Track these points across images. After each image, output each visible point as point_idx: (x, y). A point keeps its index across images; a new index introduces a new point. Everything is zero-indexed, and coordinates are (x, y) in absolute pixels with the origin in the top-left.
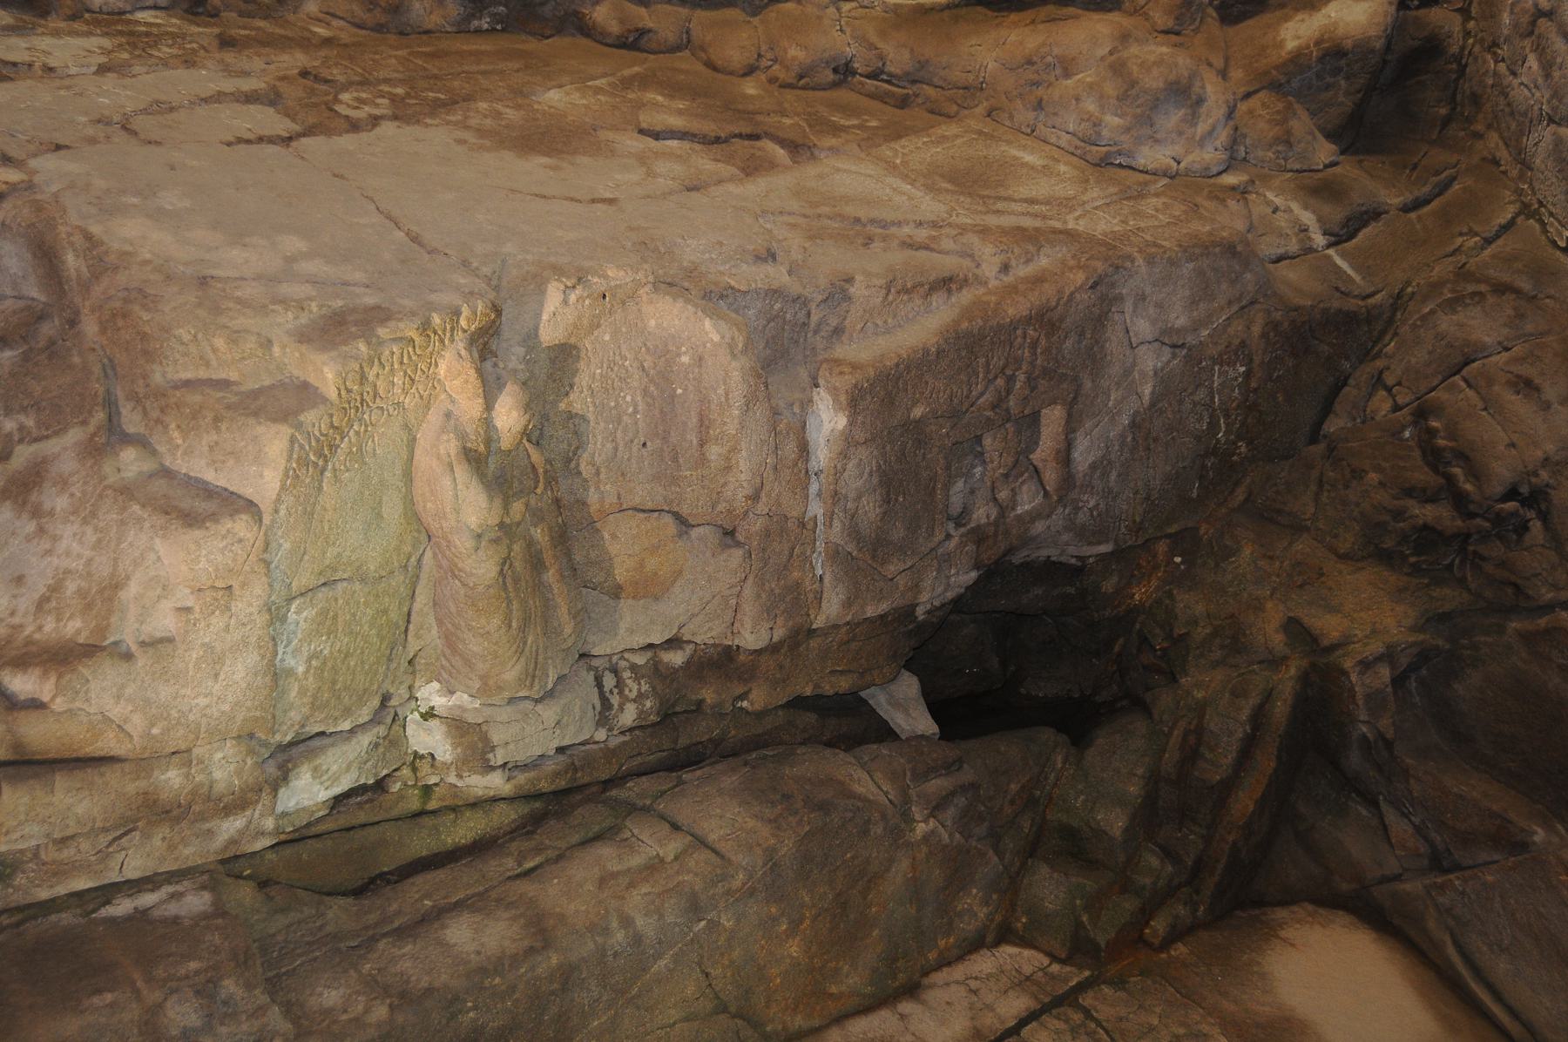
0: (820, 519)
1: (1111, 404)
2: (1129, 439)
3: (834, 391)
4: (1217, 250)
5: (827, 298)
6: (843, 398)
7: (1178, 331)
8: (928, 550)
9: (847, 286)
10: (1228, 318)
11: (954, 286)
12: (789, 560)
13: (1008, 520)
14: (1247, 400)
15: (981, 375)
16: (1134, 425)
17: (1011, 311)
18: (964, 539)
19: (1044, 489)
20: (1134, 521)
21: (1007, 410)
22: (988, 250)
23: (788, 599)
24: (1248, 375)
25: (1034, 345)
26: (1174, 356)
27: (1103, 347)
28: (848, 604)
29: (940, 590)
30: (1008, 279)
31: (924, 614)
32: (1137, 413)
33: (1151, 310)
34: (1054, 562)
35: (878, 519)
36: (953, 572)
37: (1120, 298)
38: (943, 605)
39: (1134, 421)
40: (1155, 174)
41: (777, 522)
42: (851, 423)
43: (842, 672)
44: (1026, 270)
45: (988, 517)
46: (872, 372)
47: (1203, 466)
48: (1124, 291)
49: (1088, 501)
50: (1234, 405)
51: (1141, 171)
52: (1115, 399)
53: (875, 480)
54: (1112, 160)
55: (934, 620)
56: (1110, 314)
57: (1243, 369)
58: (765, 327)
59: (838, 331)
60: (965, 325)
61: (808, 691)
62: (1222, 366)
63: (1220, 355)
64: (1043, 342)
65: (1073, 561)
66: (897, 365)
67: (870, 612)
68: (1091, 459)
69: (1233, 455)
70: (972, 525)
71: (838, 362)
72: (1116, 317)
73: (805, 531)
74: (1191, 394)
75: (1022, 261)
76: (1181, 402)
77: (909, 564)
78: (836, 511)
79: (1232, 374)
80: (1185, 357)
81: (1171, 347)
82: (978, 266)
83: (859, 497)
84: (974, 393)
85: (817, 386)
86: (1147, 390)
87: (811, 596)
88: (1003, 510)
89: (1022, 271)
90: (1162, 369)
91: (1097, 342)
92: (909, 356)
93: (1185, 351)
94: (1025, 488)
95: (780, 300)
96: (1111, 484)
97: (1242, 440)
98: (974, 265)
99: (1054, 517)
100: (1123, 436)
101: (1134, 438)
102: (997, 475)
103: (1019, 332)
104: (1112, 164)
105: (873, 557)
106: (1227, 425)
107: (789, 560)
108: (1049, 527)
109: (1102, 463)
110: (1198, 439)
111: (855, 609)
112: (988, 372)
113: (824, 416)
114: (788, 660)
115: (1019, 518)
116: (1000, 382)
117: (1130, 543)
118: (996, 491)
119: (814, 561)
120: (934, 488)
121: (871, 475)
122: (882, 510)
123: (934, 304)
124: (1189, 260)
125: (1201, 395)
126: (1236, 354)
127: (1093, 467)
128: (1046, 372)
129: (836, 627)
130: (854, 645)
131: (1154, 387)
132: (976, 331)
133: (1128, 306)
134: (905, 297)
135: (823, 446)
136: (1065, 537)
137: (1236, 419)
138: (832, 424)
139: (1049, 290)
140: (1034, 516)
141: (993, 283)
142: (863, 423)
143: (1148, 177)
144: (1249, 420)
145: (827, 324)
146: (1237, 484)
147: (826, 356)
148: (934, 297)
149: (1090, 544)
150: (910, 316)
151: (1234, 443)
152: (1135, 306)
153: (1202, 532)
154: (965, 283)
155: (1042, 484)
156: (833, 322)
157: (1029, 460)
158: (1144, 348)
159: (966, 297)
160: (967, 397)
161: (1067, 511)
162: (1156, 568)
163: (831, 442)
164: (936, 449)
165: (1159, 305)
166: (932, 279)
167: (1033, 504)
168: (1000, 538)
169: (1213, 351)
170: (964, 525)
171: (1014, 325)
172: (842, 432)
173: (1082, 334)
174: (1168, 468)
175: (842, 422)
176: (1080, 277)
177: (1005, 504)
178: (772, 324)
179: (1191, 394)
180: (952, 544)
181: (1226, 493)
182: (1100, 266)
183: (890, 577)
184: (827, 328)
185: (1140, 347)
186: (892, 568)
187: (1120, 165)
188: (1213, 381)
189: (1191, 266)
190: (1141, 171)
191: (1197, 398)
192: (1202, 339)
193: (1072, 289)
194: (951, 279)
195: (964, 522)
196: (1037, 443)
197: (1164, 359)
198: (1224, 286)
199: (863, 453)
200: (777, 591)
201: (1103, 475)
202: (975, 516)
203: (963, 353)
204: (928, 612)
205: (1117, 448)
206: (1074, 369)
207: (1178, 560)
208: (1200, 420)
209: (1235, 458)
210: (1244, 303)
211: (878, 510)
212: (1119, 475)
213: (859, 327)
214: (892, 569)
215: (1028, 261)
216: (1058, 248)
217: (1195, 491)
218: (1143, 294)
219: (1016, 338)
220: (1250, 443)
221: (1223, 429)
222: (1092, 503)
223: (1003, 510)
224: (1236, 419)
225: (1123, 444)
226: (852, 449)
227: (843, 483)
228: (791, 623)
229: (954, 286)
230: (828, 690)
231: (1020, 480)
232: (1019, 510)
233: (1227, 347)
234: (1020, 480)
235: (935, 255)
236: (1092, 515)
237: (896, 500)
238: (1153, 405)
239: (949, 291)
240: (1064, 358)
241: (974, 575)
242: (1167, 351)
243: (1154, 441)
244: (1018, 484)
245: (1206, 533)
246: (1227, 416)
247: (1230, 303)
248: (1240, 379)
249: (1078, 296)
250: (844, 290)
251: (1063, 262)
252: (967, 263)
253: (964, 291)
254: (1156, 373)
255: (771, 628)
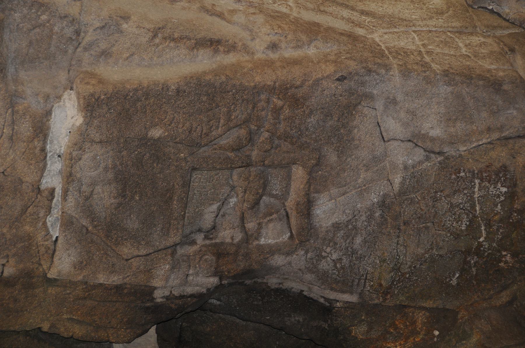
0: (58, 192)
1: (360, 181)
2: (377, 214)
3: (78, 94)
4: (481, 83)
5: (103, 27)
6: (82, 102)
7: (433, 140)
8: (162, 246)
9: (122, 22)
10: (490, 143)
11: (221, 48)
12: (21, 215)
13: (250, 246)
14: (509, 217)
15: (222, 121)
16: (383, 204)
17: (258, 79)
18: (204, 249)
19: (291, 233)
20: (381, 285)
21: (249, 157)
22: (266, 29)
23: (19, 245)
24: (511, 196)
25: (277, 111)
26: (428, 159)
27: (350, 131)
28: (79, 266)
29: (177, 282)
30: (273, 56)
31: (162, 298)
32: (385, 196)
33: (402, 115)
34: (305, 296)
35: (113, 206)
36: (191, 272)
37: (370, 97)
38: (182, 297)
39: (384, 202)
40: (513, 23)
41: (11, 181)
42: (88, 123)
43: (79, 322)
44: (293, 53)
45: (232, 238)
46: (110, 90)
47: (465, 262)
48: (375, 92)
49: (330, 253)
50: (496, 217)
51: (505, 19)
52: (364, 178)
53: (110, 175)
54: (487, 6)
55: (173, 306)
56: (359, 107)
57: (504, 190)
58: (30, 30)
59: (105, 54)
60: (208, 78)
61: (46, 327)
62: (482, 180)
63: (480, 171)
64: (287, 112)
65: (322, 300)
66: (136, 90)
67: (102, 279)
68: (334, 219)
69: (501, 261)
70: (217, 241)
71: (92, 75)
72: (366, 111)
73: (39, 196)
74: (448, 196)
75: (292, 45)
76: (435, 200)
77: (143, 252)
78: (71, 188)
79: (492, 190)
80: (440, 163)
81: (425, 150)
82: (253, 39)
83: (93, 184)
84: (214, 133)
85: (72, 89)
86: (397, 180)
87: (42, 250)
88: (248, 238)
89: (289, 53)
90: (413, 167)
91: (344, 126)
92: (148, 87)
93: (442, 158)
94: (271, 225)
95: (47, 13)
96: (355, 247)
97: (505, 250)
98: (249, 38)
99: (295, 256)
100: (371, 211)
101: (382, 216)
102: (244, 208)
103: (263, 97)
104: (486, 8)
105: (107, 236)
106: (488, 233)
107: (21, 215)
108: (290, 263)
109: (347, 226)
110: (457, 236)
111: (85, 273)
112: (229, 120)
113: (68, 113)
114: (23, 296)
115: (260, 247)
116: (243, 132)
117: (376, 301)
118: (245, 221)
119: (49, 224)
120: (171, 198)
121: (106, 169)
122: (117, 201)
123: (200, 57)
124: (449, 84)
125: (458, 199)
126: (497, 175)
127: (337, 226)
128: (286, 137)
129: (73, 284)
130: (89, 303)
131: (404, 179)
132: (217, 84)
133: (379, 105)
134: (172, 44)
135: (64, 135)
136: (309, 277)
137: (498, 230)
138: (73, 120)
139: (297, 72)
140: (274, 250)
141: (259, 56)
142: (99, 127)
143: (507, 24)
144: (514, 235)
145: (98, 46)
146: (505, 288)
147: (89, 70)
148: (201, 52)
149: (332, 289)
150: (175, 60)
151: (499, 251)
152: (386, 107)
153: (459, 316)
154: (232, 48)
155: (290, 227)
156: (103, 45)
157: (285, 206)
158: (396, 143)
159: (231, 59)
160: (207, 135)
161: (309, 255)
162: (415, 333)
163: (71, 133)
164: (174, 167)
165: (413, 113)
166: (199, 36)
167: (276, 241)
168: (240, 258)
169: (476, 167)
170: (211, 239)
171: (257, 90)
172: (79, 128)
173: (328, 115)
174: (421, 251)
175: (79, 120)
176: (330, 69)
177: (250, 233)
178: (37, 30)
179: (448, 196)
180: (191, 250)
181: (492, 292)
182: (353, 65)
183: (125, 257)
184: (97, 49)
185: (391, 142)
186: (126, 250)
187: (492, 11)
188: (474, 193)
189: (449, 89)
190: (505, 19)
191: (454, 201)
192: (463, 153)
193: (320, 76)
194: (219, 42)
195: (211, 236)
196: (288, 194)
197: (417, 159)
198: (484, 115)
199: (98, 150)
200: (8, 236)
201: (348, 237)
202: (221, 234)
203: (204, 98)
204: (167, 298)
205: (364, 218)
206: (316, 141)
207: (437, 333)
208: (459, 220)
209: (502, 264)
210: (506, 134)
211: (113, 201)
212: (365, 241)
213: (125, 56)
214: (126, 250)
215: (297, 47)
216: (329, 45)
217: (454, 279)
218: (394, 99)
219: (260, 101)
220: (514, 255)
221: (484, 235)
222: (335, 256)
223: (248, 238)
224: (498, 230)
225: (370, 217)
226: (87, 145)
227: (78, 169)
228: (21, 266)
229: (221, 48)
230: (62, 331)
231: (268, 218)
232: (262, 241)
233: (488, 166)
234: (268, 218)
235: (224, 23)
236: (335, 266)
237: (132, 198)
238: (402, 193)
239: (216, 51)
240: (307, 129)
241: (214, 281)
242: (419, 154)
243: (405, 224)
244: (266, 220)
245: (462, 318)
246: (488, 225)
247: (489, 129)
248: (502, 198)
249: (325, 83)
250: (118, 25)
251: (326, 56)
252: (245, 35)
253: (231, 55)
254: (406, 168)
255: (3, 265)
